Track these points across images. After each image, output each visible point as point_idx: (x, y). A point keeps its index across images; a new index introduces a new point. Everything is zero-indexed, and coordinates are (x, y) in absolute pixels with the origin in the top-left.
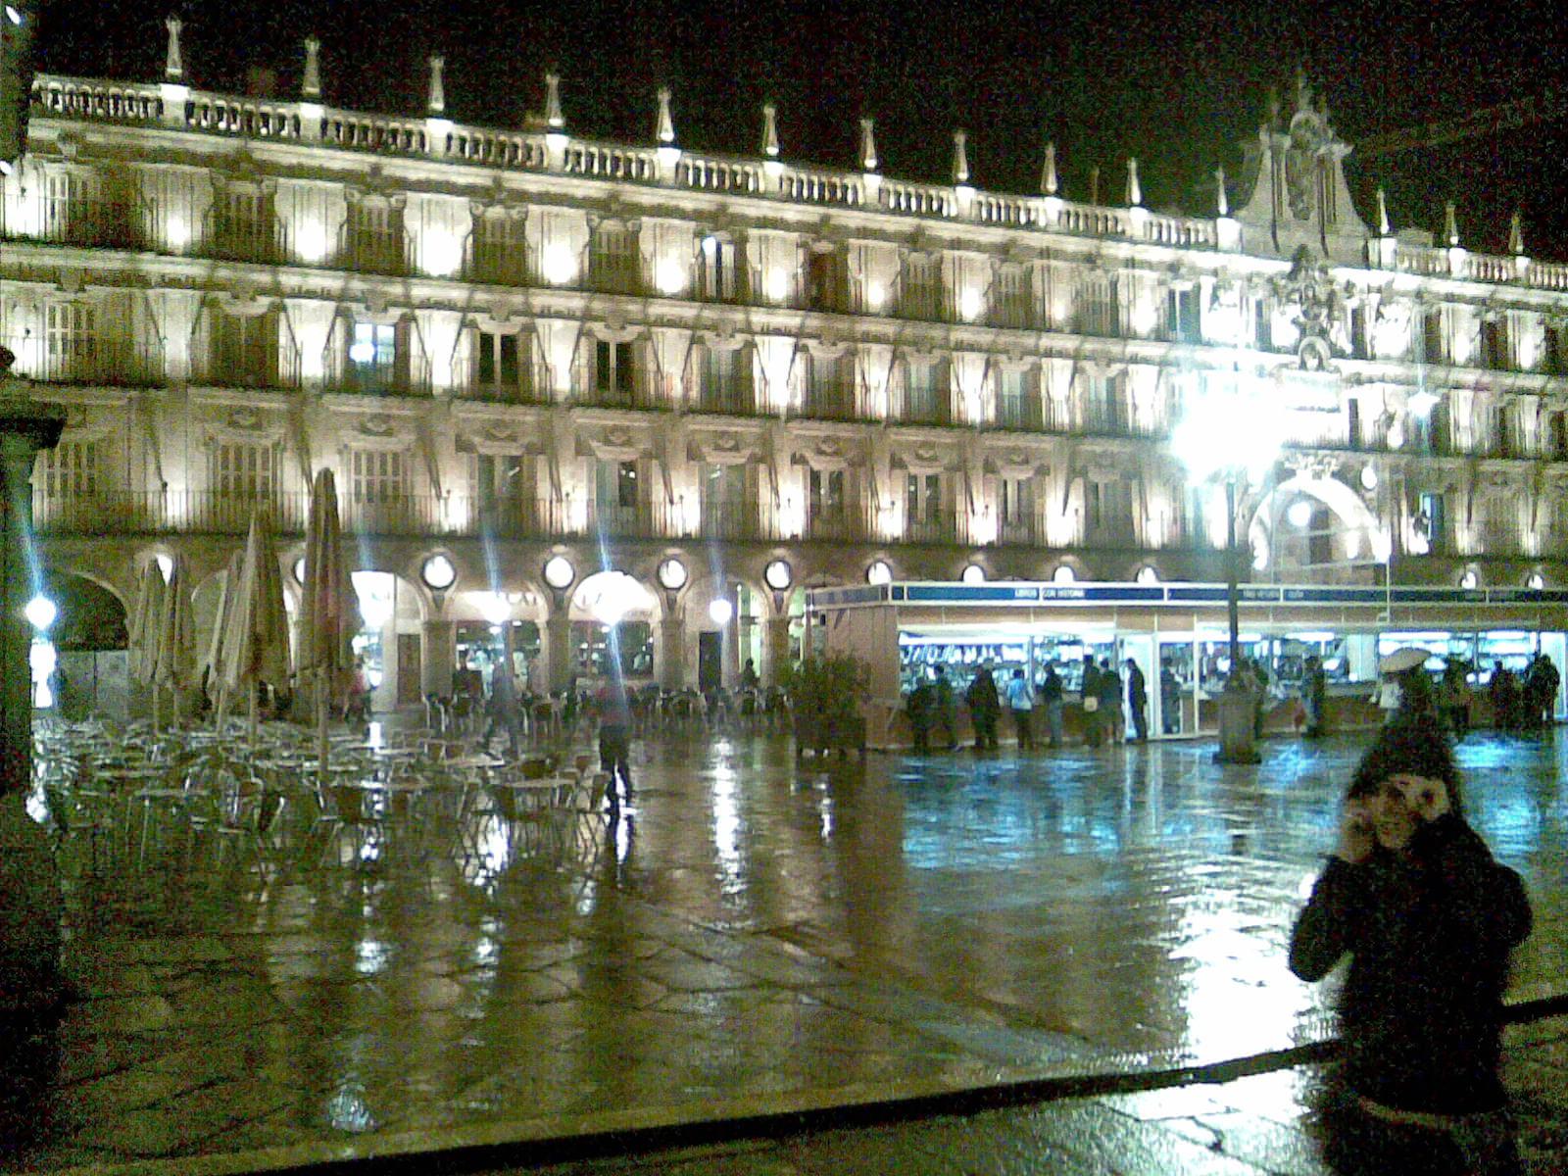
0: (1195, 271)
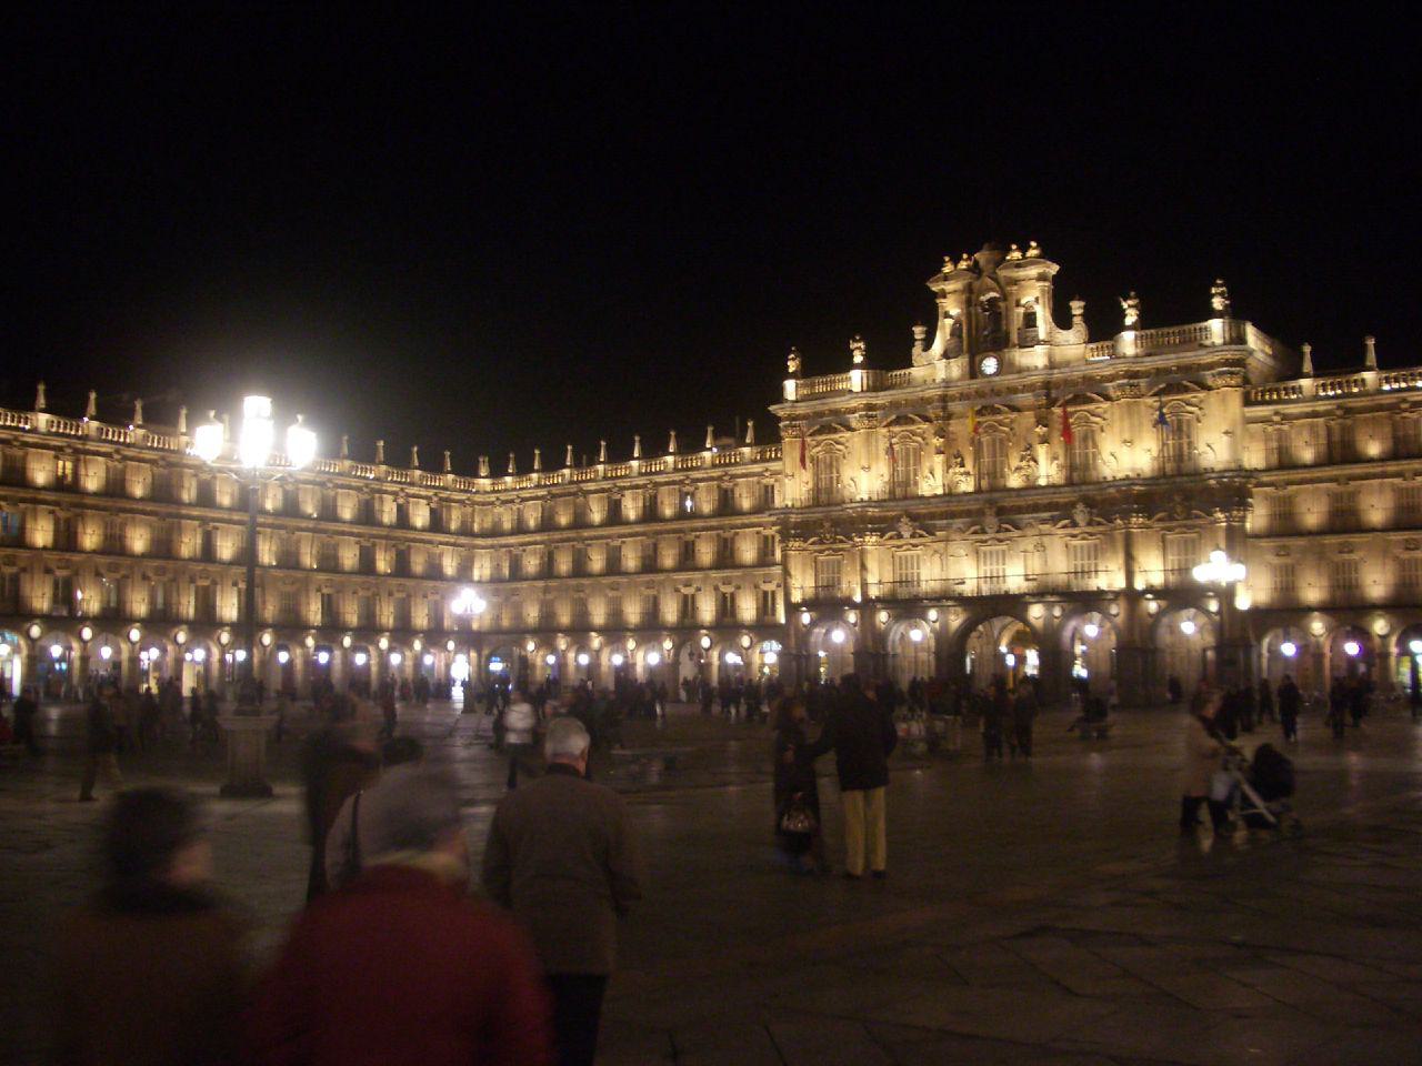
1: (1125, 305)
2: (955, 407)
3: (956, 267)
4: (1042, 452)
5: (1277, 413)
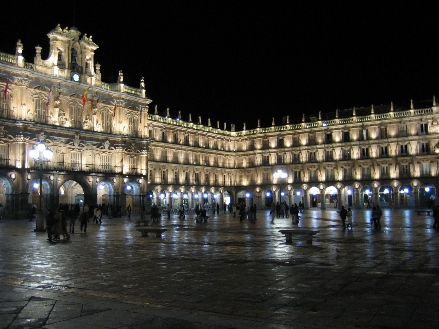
0: (427, 119)
1: (120, 74)
2: (63, 90)
3: (63, 30)
4: (95, 117)
5: (151, 123)
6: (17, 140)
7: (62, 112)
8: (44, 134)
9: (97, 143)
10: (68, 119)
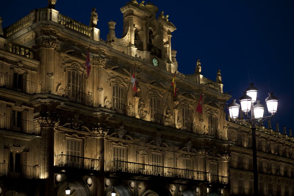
6: (94, 134)
7: (142, 103)
8: (124, 129)
9: (179, 144)
10: (148, 112)
